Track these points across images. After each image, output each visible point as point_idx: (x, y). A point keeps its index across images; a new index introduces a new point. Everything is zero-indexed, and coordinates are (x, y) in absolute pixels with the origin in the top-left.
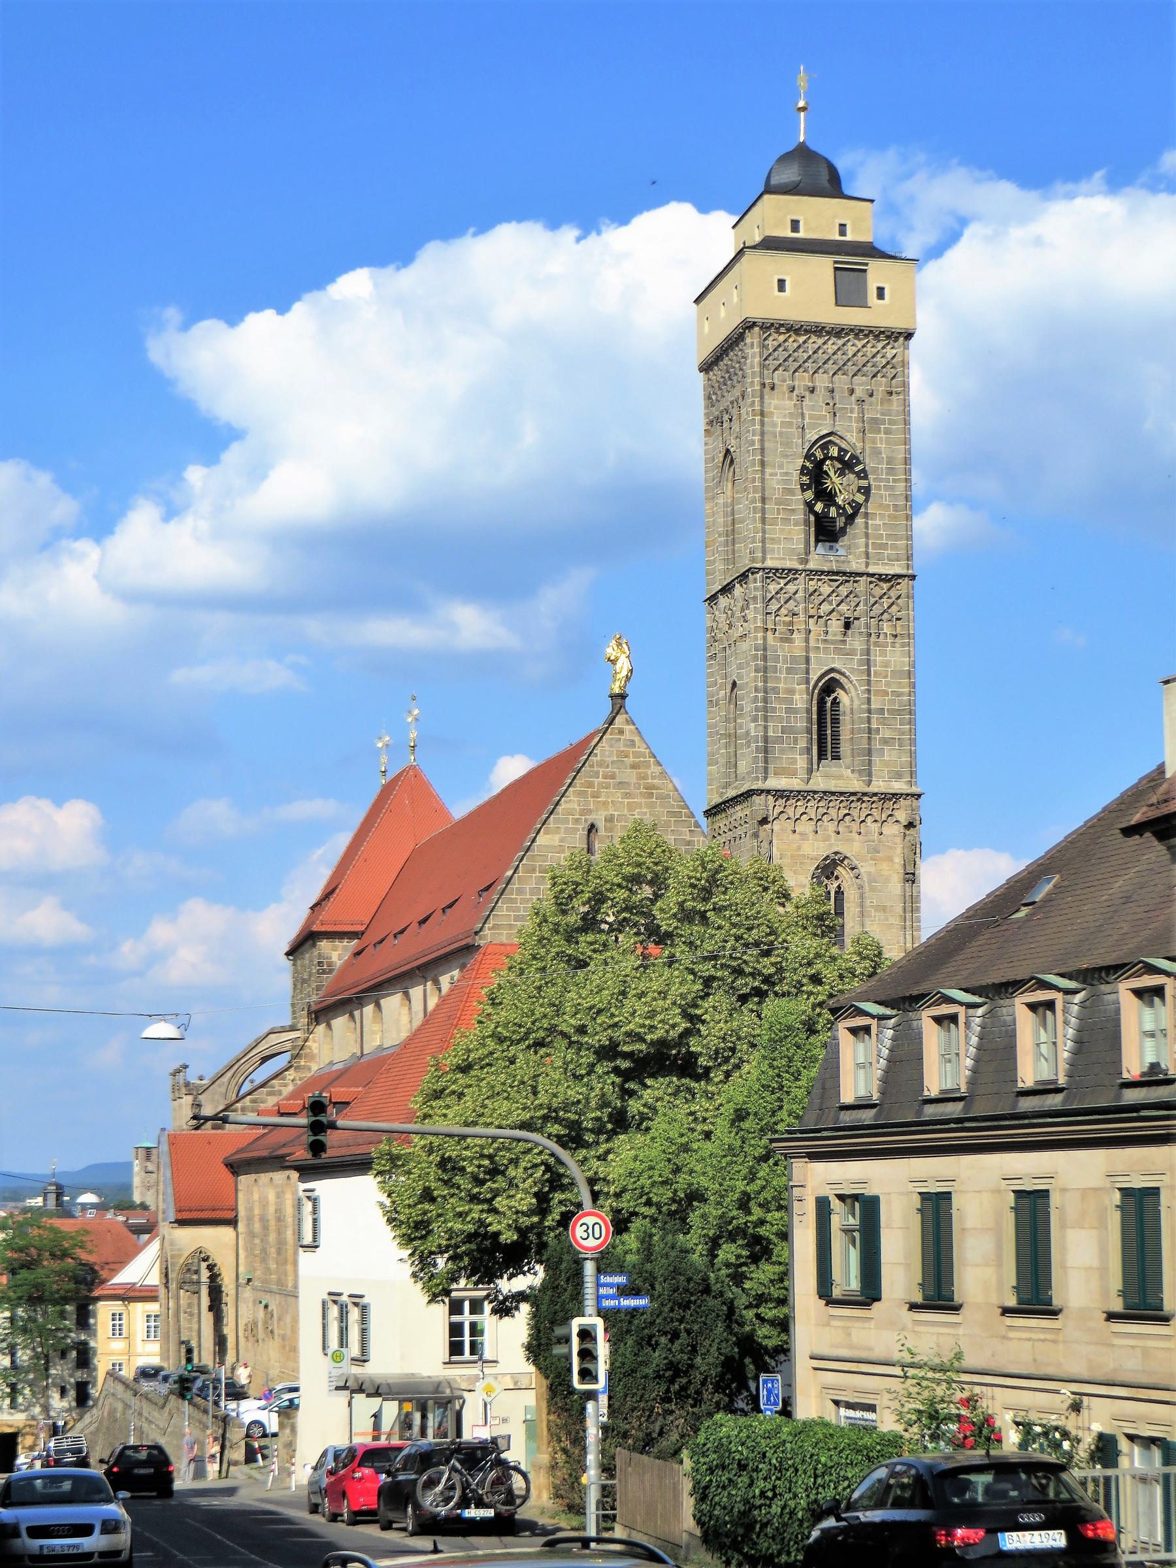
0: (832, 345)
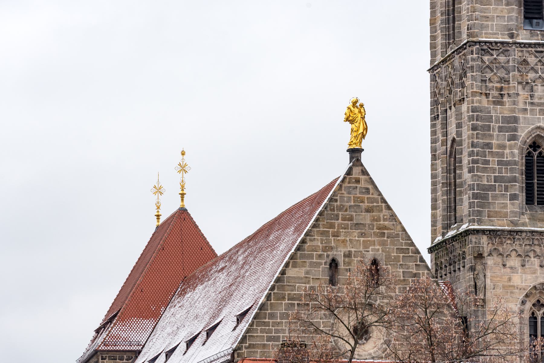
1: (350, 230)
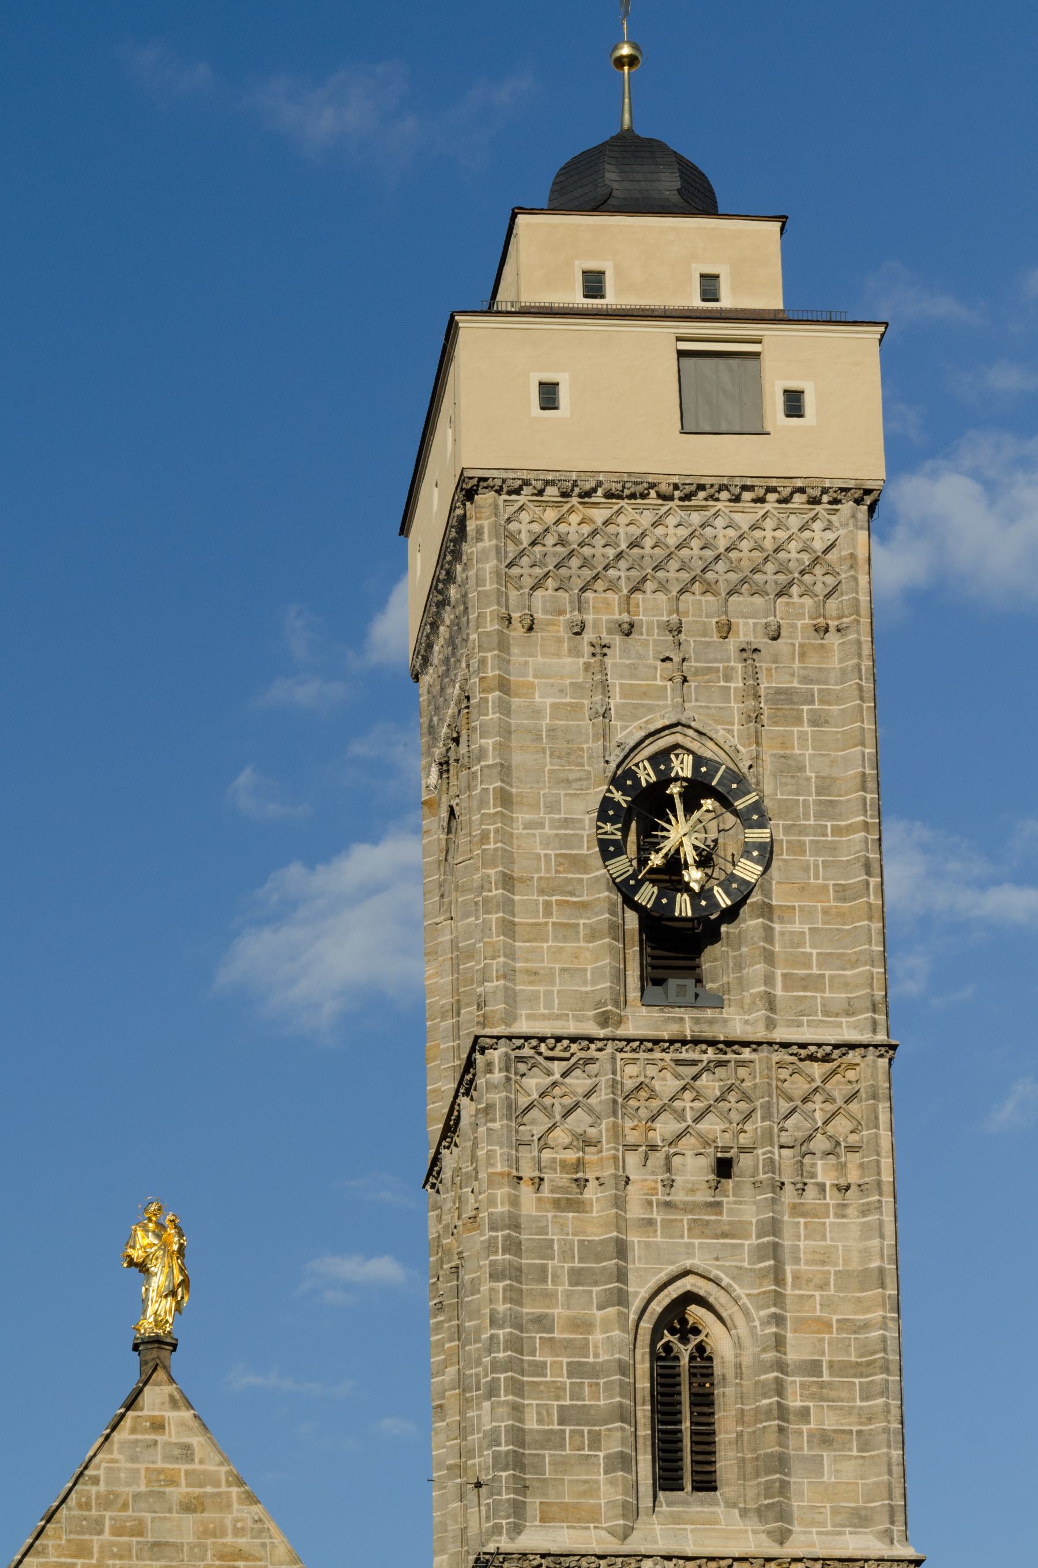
0: (675, 525)
1: (135, 1562)
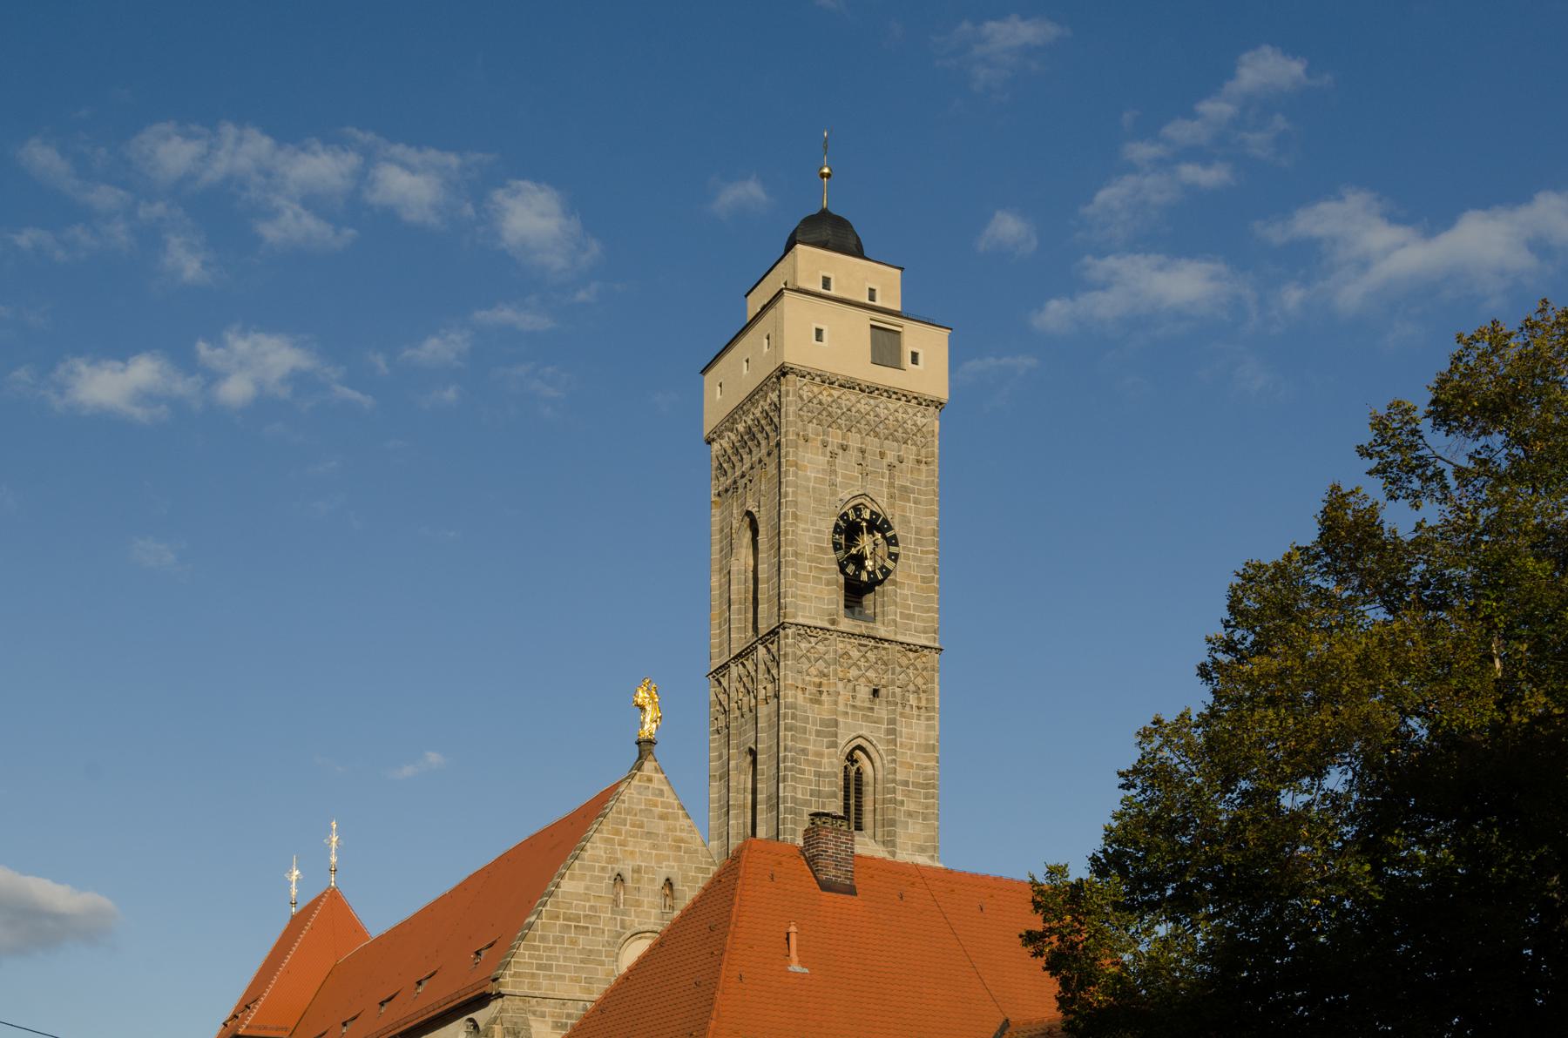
0: (864, 404)
